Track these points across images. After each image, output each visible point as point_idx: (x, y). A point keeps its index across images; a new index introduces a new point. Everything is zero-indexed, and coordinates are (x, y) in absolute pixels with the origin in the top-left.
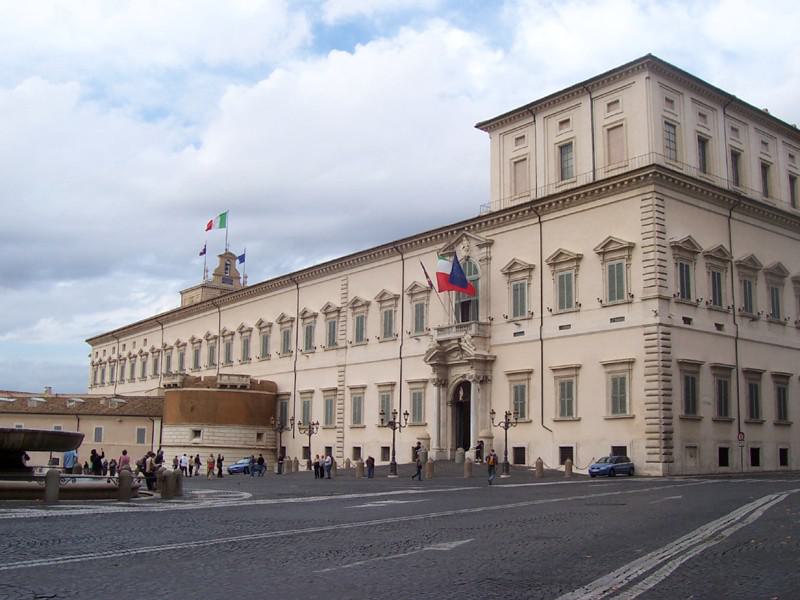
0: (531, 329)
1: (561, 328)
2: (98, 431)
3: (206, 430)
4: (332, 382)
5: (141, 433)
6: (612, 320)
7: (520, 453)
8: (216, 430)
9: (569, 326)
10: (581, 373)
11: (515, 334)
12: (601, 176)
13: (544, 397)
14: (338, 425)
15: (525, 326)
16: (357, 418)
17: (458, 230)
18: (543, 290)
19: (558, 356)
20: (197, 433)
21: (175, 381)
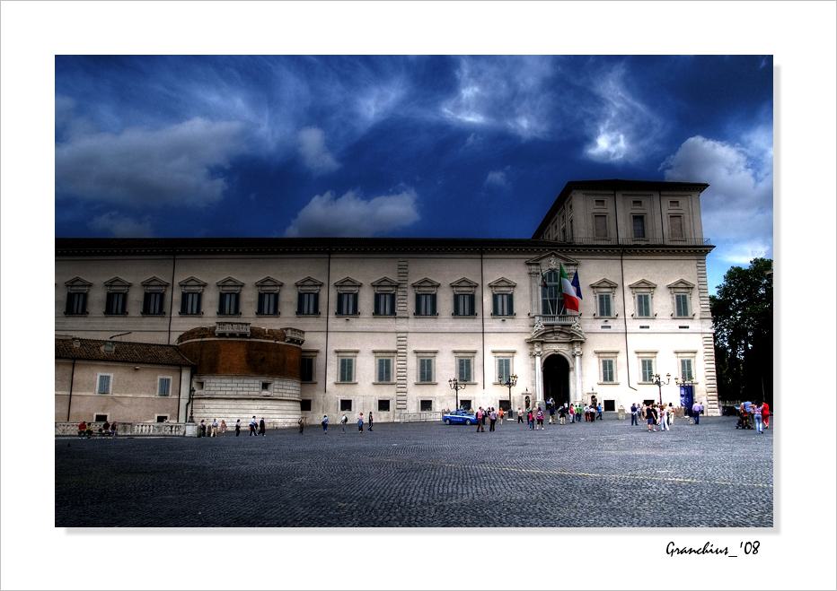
0: (616, 325)
1: (642, 327)
2: (105, 380)
3: (276, 382)
4: (389, 343)
5: (165, 384)
6: (680, 327)
7: (610, 405)
8: (284, 383)
9: (648, 327)
10: (657, 355)
11: (602, 327)
12: (667, 242)
13: (627, 369)
14: (401, 382)
15: (610, 323)
16: (426, 376)
17: (550, 250)
18: (626, 303)
19: (639, 342)
20: (265, 386)
21: (243, 331)
